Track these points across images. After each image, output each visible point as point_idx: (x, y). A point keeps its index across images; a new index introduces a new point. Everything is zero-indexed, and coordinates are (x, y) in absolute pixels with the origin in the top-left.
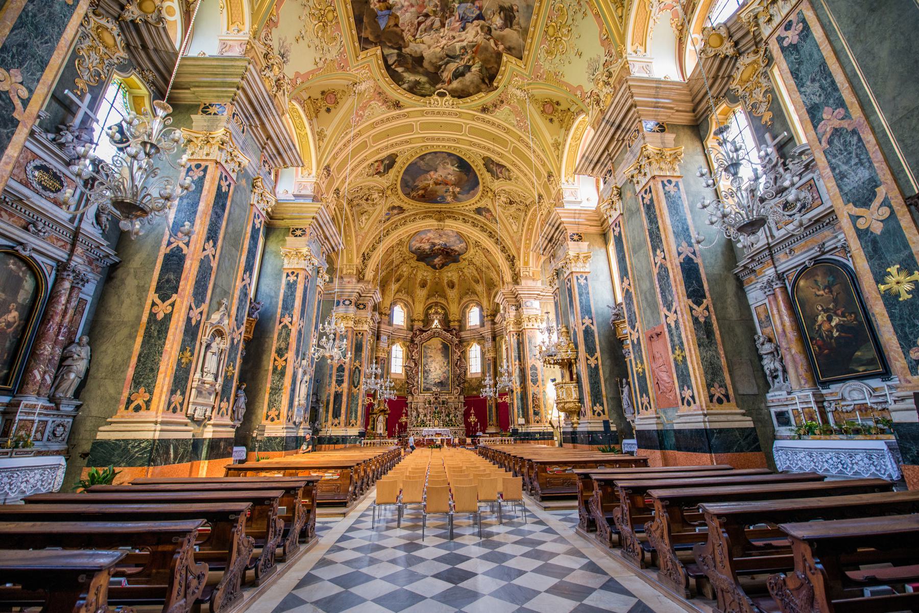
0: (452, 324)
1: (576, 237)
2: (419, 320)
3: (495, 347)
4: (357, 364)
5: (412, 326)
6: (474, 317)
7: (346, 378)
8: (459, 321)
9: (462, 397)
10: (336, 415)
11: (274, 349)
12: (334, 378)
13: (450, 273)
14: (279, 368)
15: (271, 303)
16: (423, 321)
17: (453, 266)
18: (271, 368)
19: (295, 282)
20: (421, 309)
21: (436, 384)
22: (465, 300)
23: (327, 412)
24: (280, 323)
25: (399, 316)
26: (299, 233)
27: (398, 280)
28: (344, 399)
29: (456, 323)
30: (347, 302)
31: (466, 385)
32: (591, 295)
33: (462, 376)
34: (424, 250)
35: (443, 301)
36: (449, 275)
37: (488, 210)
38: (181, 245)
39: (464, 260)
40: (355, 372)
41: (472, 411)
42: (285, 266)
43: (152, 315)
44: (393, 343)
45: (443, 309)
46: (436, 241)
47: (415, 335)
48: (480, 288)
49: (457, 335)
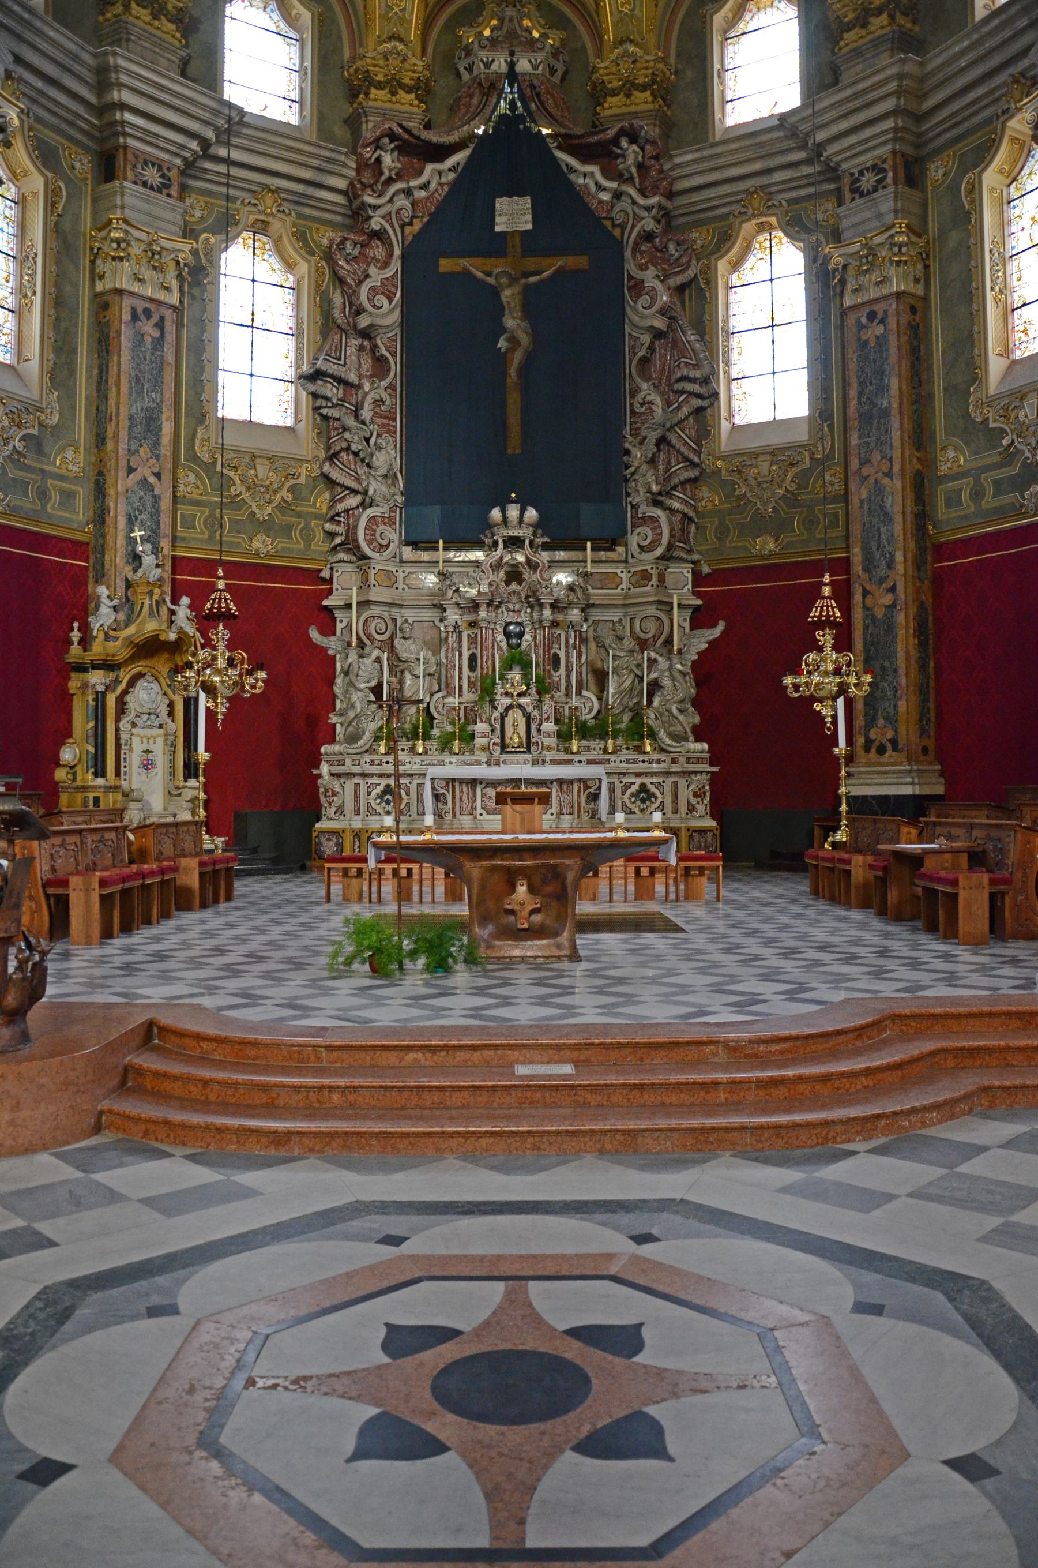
0: (614, 105)
5: (353, 123)
8: (662, 90)
9: (681, 575)
16: (423, 90)
29: (643, 100)
31: (708, 497)
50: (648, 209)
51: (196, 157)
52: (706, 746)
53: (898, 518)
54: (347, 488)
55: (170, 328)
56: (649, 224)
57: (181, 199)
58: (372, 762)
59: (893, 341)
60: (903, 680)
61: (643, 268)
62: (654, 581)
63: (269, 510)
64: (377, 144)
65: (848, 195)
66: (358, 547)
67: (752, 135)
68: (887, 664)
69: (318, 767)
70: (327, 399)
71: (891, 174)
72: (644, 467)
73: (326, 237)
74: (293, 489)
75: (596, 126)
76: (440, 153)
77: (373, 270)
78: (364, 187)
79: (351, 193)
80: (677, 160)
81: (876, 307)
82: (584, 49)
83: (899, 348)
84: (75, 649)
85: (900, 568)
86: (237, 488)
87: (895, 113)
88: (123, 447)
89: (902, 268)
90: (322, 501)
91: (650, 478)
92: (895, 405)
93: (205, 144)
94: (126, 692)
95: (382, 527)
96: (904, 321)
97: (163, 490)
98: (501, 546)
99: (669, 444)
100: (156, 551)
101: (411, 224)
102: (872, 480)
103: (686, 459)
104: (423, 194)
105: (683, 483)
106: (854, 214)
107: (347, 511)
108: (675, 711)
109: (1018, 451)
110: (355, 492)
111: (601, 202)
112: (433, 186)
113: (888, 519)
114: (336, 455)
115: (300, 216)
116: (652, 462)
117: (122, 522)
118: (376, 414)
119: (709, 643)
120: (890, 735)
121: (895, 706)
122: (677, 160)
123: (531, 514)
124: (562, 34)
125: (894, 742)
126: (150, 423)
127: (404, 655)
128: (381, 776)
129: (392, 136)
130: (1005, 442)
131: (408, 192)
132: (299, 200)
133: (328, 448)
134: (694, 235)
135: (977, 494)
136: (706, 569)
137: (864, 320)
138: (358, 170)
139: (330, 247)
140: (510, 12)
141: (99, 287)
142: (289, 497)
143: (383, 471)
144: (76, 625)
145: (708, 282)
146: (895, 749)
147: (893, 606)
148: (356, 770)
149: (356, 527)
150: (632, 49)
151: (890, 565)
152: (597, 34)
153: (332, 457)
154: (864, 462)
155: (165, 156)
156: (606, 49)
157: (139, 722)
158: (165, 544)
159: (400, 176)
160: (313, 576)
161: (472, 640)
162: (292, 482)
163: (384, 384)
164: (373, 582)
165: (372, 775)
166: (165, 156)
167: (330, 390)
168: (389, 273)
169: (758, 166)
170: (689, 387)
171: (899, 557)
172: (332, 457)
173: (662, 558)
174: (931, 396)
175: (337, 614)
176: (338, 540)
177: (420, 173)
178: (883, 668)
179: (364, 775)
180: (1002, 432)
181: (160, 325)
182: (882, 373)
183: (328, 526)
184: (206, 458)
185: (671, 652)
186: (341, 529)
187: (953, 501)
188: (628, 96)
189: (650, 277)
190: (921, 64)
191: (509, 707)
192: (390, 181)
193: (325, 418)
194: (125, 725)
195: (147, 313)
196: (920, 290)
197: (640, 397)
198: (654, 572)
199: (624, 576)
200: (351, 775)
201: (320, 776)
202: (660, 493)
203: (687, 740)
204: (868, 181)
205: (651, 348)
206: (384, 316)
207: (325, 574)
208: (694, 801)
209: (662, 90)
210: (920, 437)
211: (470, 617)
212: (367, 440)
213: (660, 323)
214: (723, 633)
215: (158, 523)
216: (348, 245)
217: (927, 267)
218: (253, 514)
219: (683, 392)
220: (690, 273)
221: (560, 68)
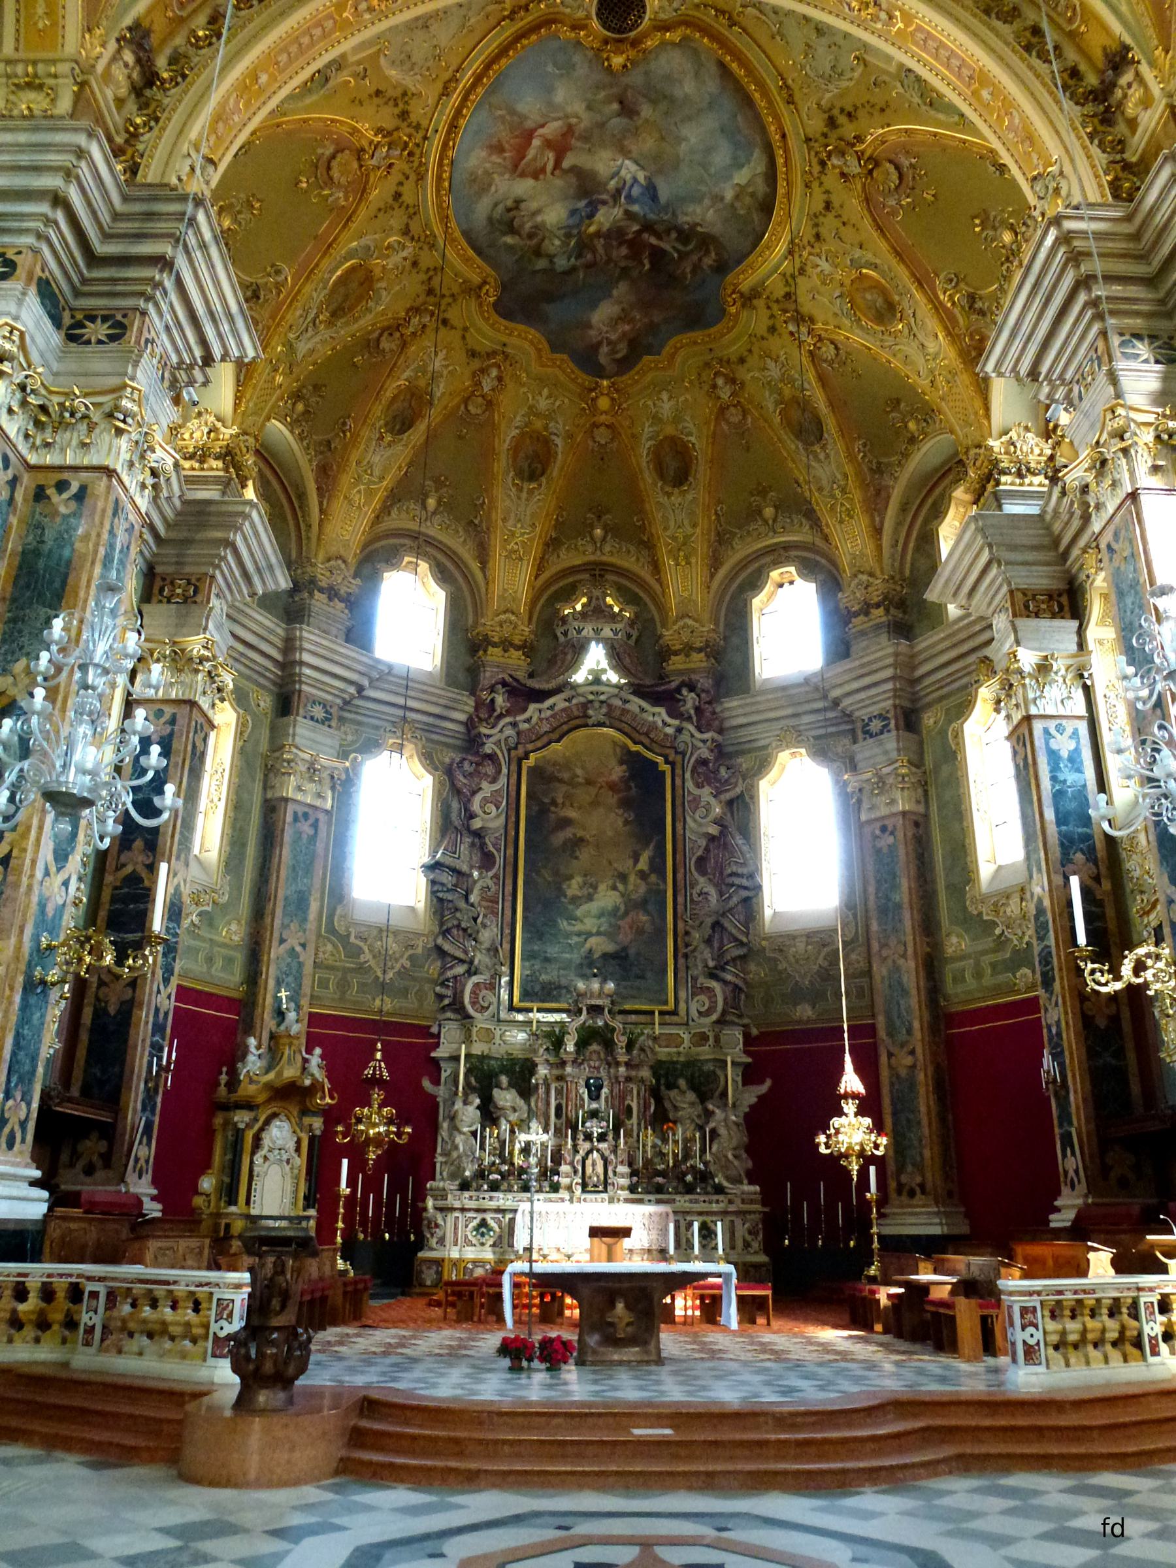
0: (676, 663)
2: (506, 645)
5: (473, 672)
6: (790, 631)
8: (715, 652)
13: (668, 400)
16: (528, 649)
17: (685, 351)
20: (524, 595)
21: (591, 965)
22: (741, 550)
27: (401, 424)
33: (732, 925)
35: (630, 562)
39: (748, 299)
41: (851, 1081)
46: (603, 163)
47: (486, 711)
50: (704, 741)
51: (353, 697)
52: (758, 1188)
53: (914, 992)
54: (456, 958)
55: (322, 827)
56: (704, 753)
57: (338, 729)
58: (471, 1198)
59: (902, 851)
60: (926, 1131)
61: (699, 786)
62: (711, 1041)
63: (390, 975)
64: (492, 689)
65: (860, 735)
66: (463, 1008)
67: (784, 691)
68: (911, 1116)
69: (424, 1200)
70: (443, 884)
71: (893, 722)
72: (702, 946)
73: (448, 757)
74: (411, 958)
75: (662, 678)
76: (540, 696)
77: (485, 785)
78: (481, 720)
79: (470, 724)
80: (727, 705)
81: (886, 822)
82: (653, 620)
83: (907, 854)
84: (222, 1090)
85: (918, 1034)
86: (367, 956)
87: (893, 678)
88: (277, 923)
89: (906, 793)
90: (433, 968)
91: (707, 954)
92: (906, 900)
93: (360, 689)
94: (262, 1129)
95: (484, 992)
96: (910, 834)
97: (307, 958)
98: (585, 1012)
99: (723, 928)
100: (298, 1008)
101: (516, 748)
102: (890, 961)
103: (736, 939)
104: (526, 726)
105: (734, 959)
106: (866, 751)
107: (455, 977)
108: (730, 1156)
109: (1008, 940)
110: (462, 961)
111: (666, 735)
112: (534, 720)
113: (905, 992)
114: (448, 931)
115: (428, 740)
116: (708, 941)
117: (271, 983)
118: (483, 899)
119: (759, 1097)
120: (919, 1179)
121: (921, 1154)
122: (727, 705)
123: (611, 986)
124: (635, 608)
125: (922, 1186)
126: (300, 903)
127: (501, 1103)
128: (477, 1210)
129: (504, 684)
130: (998, 931)
131: (514, 725)
132: (429, 729)
133: (441, 924)
134: (739, 760)
135: (978, 975)
136: (755, 1032)
137: (878, 832)
138: (477, 708)
139: (451, 764)
140: (597, 593)
141: (269, 795)
142: (408, 964)
143: (486, 945)
144: (224, 1069)
145: (752, 797)
146: (923, 1192)
147: (914, 1067)
148: (457, 1205)
149: (462, 992)
150: (690, 622)
151: (909, 1031)
152: (662, 608)
153: (445, 933)
154: (883, 945)
155: (329, 697)
156: (670, 621)
157: (271, 1156)
158: (305, 1002)
159: (509, 712)
160: (424, 1031)
161: (559, 1092)
162: (411, 952)
163: (490, 874)
164: (475, 1038)
165: (469, 1210)
166: (329, 697)
168: (496, 787)
169: (789, 711)
170: (737, 881)
171: (916, 1025)
172: (445, 933)
173: (718, 1022)
174: (935, 892)
175: (442, 1064)
176: (446, 1002)
177: (525, 710)
178: (908, 1120)
179: (463, 1210)
180: (995, 924)
181: (315, 825)
182: (894, 876)
183: (438, 989)
184: (342, 931)
185: (726, 1105)
186: (449, 993)
187: (959, 979)
188: (687, 656)
189: (706, 793)
190: (911, 647)
191: (590, 1152)
192: (501, 716)
193: (441, 900)
194: (258, 1159)
195: (306, 816)
196: (921, 809)
197: (698, 889)
198: (711, 1034)
199: (686, 1037)
200: (453, 1209)
201: (425, 1209)
202: (715, 968)
203: (741, 1183)
204: (876, 725)
205: (707, 849)
206: (492, 820)
207: (434, 1030)
208: (749, 1238)
210: (928, 926)
211: (556, 1072)
212: (475, 919)
213: (714, 830)
214: (770, 1089)
215: (300, 985)
216: (466, 765)
217: (926, 792)
218: (377, 978)
219: (732, 885)
220: (738, 790)
221: (635, 634)
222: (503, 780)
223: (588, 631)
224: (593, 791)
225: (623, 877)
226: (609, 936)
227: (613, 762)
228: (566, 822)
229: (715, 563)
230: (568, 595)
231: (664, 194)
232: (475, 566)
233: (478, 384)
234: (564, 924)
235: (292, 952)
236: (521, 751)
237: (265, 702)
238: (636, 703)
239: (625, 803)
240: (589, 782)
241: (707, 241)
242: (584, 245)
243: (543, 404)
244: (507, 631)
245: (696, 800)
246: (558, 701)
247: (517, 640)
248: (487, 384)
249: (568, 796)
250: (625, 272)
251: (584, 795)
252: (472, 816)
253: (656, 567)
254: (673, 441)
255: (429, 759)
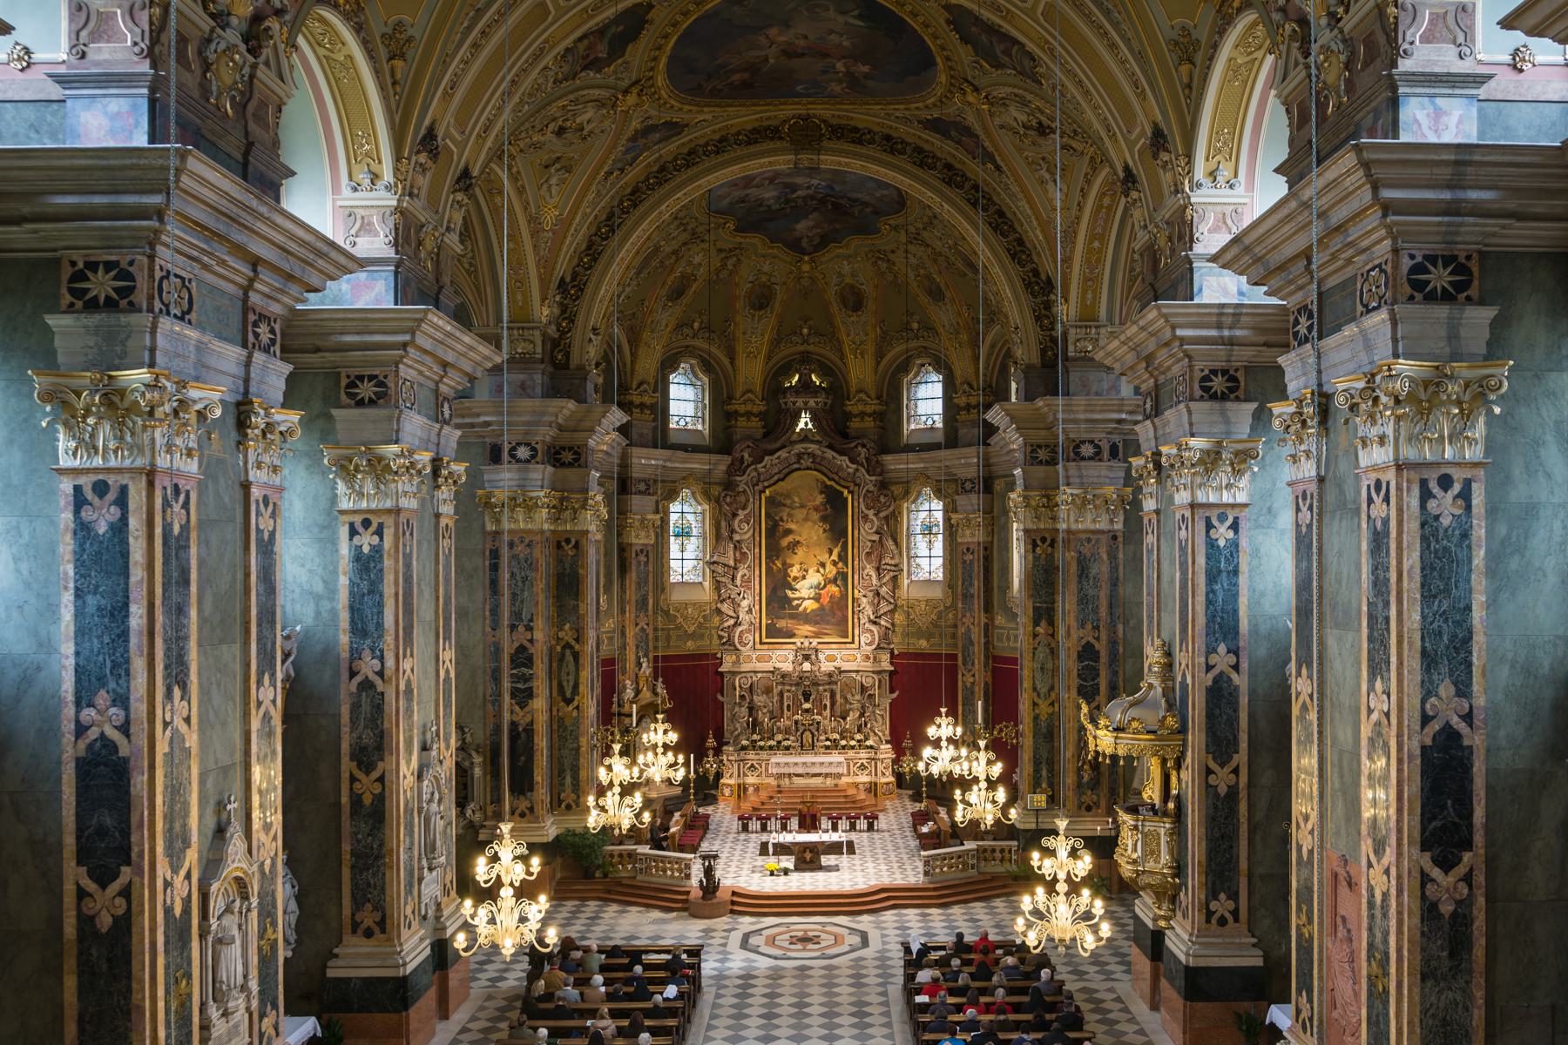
0: (855, 424)
1: (1218, 384)
2: (748, 414)
3: (988, 511)
4: (567, 634)
6: (927, 402)
7: (541, 687)
8: (879, 416)
10: (522, 783)
11: (345, 747)
12: (506, 684)
13: (846, 263)
14: (367, 800)
15: (318, 613)
18: (345, 799)
19: (377, 550)
20: (758, 380)
23: (495, 773)
24: (353, 674)
25: (685, 402)
26: (366, 390)
27: (677, 293)
28: (542, 743)
29: (869, 423)
30: (523, 452)
31: (899, 618)
32: (1243, 580)
34: (760, 202)
36: (846, 268)
37: (968, 131)
38: (115, 735)
39: (895, 228)
40: (562, 658)
42: (345, 504)
43: (86, 922)
44: (672, 495)
45: (825, 371)
46: (799, 180)
47: (737, 468)
48: (943, 316)
49: (873, 467)
75: (845, 436)
76: (772, 453)
84: (615, 706)
97: (650, 630)
106: (962, 500)
167: (720, 569)
189: (871, 513)
209: (879, 416)
222: (750, 507)
223: (800, 403)
224: (805, 511)
225: (823, 565)
226: (817, 598)
227: (816, 493)
228: (788, 532)
229: (879, 356)
230: (786, 370)
231: (837, 188)
232: (726, 361)
233: (724, 266)
234: (789, 593)
235: (643, 629)
236: (760, 487)
237: (614, 486)
238: (830, 454)
239: (824, 519)
240: (802, 506)
241: (866, 204)
242: (787, 202)
243: (766, 268)
244: (749, 408)
245: (866, 517)
246: (783, 454)
247: (755, 410)
248: (730, 263)
249: (789, 515)
250: (815, 210)
251: (800, 514)
252: (733, 531)
253: (842, 357)
254: (852, 287)
255: (707, 496)
